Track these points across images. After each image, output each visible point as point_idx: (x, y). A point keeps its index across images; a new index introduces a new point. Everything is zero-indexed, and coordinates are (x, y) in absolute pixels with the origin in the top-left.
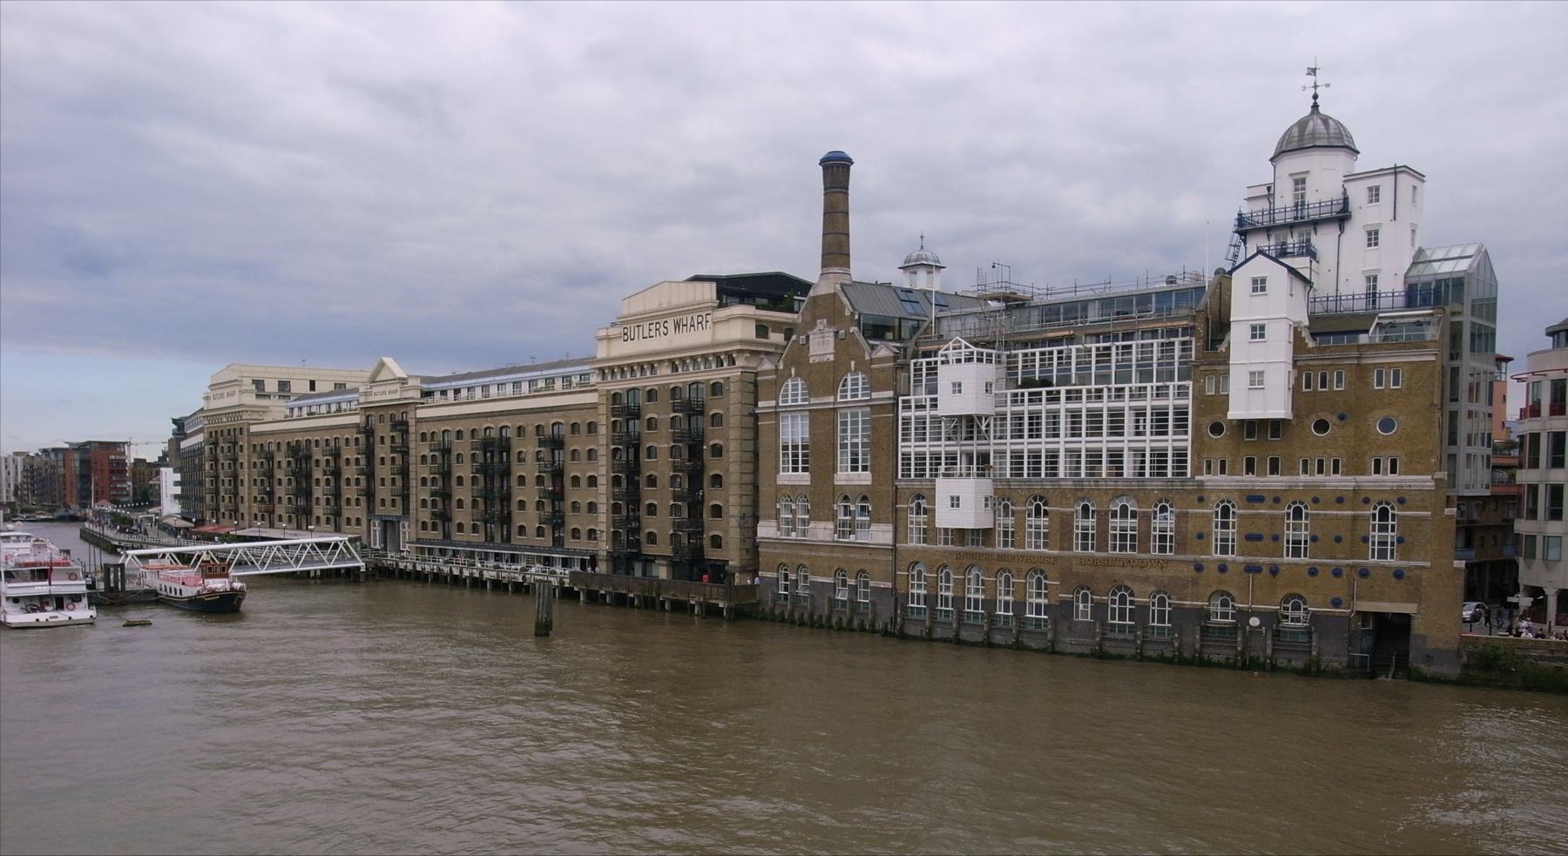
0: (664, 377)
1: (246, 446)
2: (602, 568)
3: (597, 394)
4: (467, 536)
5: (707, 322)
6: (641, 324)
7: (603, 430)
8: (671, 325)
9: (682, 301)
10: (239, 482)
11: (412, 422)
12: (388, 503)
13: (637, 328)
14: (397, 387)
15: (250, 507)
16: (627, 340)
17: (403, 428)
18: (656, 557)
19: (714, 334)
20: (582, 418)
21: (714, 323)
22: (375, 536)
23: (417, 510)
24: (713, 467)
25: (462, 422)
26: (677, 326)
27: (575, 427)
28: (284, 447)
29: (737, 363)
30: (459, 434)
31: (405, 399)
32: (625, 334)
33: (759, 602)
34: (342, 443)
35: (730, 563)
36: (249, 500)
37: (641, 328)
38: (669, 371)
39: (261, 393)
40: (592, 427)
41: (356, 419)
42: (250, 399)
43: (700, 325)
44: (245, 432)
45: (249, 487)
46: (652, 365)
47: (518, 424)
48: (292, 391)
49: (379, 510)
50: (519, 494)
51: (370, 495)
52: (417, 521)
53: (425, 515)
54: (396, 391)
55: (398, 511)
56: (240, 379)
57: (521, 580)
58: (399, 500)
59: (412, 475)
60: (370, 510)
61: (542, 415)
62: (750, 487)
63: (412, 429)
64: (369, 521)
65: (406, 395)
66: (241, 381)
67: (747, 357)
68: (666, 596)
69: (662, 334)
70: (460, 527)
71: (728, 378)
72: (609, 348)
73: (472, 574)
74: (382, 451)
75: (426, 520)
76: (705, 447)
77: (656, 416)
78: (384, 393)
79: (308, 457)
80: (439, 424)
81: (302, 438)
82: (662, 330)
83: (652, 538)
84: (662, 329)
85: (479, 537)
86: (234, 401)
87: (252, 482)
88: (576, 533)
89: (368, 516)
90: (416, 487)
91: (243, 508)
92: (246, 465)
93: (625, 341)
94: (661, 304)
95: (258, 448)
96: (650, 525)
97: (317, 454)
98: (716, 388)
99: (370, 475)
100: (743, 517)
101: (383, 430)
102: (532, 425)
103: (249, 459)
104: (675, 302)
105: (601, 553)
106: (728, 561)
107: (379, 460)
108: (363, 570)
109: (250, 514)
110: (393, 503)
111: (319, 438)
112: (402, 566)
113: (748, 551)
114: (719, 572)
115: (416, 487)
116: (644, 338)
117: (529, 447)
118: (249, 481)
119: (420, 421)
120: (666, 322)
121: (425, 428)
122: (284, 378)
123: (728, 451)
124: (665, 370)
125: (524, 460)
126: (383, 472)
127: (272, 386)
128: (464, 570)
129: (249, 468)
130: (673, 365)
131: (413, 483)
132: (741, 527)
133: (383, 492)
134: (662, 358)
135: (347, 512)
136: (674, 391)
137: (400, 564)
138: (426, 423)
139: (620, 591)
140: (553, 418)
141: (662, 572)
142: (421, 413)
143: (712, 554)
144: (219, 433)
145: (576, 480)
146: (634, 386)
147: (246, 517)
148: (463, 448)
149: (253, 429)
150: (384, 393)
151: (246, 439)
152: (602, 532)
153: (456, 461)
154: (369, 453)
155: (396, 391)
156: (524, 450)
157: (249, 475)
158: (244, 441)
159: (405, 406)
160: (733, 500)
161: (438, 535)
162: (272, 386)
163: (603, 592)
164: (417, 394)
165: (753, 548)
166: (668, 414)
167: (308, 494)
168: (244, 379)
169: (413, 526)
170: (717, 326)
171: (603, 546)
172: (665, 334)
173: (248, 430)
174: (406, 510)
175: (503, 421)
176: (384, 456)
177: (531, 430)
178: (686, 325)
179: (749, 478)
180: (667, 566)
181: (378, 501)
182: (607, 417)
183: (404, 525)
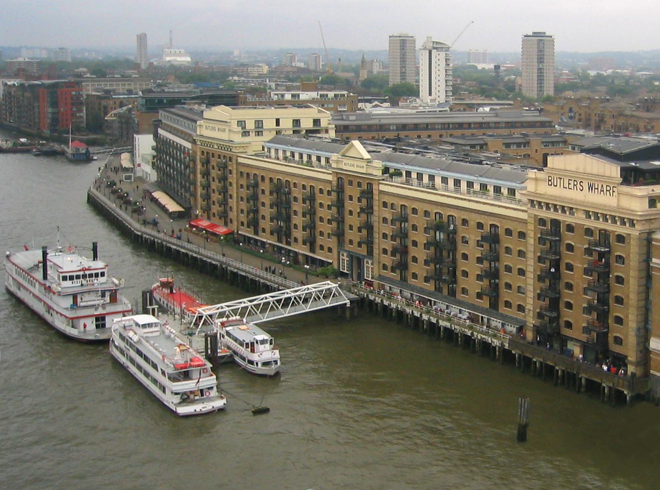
0: (578, 219)
1: (234, 171)
2: (530, 335)
3: (527, 214)
4: (419, 283)
5: (613, 192)
6: (563, 177)
7: (531, 241)
8: (585, 186)
9: (595, 172)
10: (229, 197)
11: (375, 192)
13: (559, 180)
15: (238, 216)
16: (551, 185)
17: (370, 196)
18: (572, 339)
19: (618, 201)
20: (516, 228)
21: (618, 194)
22: (343, 263)
23: (379, 254)
24: (617, 290)
25: (417, 203)
26: (591, 187)
27: (509, 232)
28: (267, 181)
29: (636, 227)
30: (415, 211)
31: (369, 174)
33: (648, 392)
34: (317, 191)
35: (629, 358)
36: (237, 211)
37: (562, 180)
39: (246, 133)
40: (522, 235)
41: (330, 178)
42: (238, 138)
43: (608, 192)
44: (234, 161)
45: (237, 202)
46: (571, 209)
47: (462, 217)
48: (264, 128)
49: (348, 247)
50: (462, 265)
51: (340, 235)
52: (379, 263)
53: (388, 260)
54: (363, 167)
55: (363, 251)
56: (229, 121)
57: (470, 335)
59: (376, 229)
61: (483, 216)
62: (644, 309)
63: (376, 197)
64: (339, 253)
65: (370, 171)
66: (230, 123)
67: (643, 224)
68: (582, 375)
69: (578, 189)
70: (415, 276)
71: (629, 234)
72: (536, 186)
73: (429, 319)
74: (353, 205)
75: (386, 263)
76: (611, 276)
77: (573, 244)
79: (289, 193)
81: (284, 179)
83: (569, 325)
85: (430, 286)
86: (224, 136)
87: (240, 199)
88: (508, 304)
89: (338, 249)
90: (379, 238)
91: (233, 215)
92: (235, 185)
93: (549, 185)
94: (577, 169)
95: (245, 175)
96: (567, 315)
97: (297, 193)
98: (621, 238)
99: (340, 220)
100: (639, 329)
101: (352, 191)
102: (474, 221)
103: (237, 182)
104: (588, 170)
105: (528, 324)
106: (627, 357)
107: (348, 212)
108: (348, 305)
109: (238, 221)
110: (360, 245)
111: (297, 182)
112: (372, 297)
113: (641, 352)
114: (620, 361)
115: (379, 238)
116: (564, 187)
117: (474, 236)
118: (237, 197)
119: (381, 192)
120: (582, 182)
121: (386, 199)
122: (259, 118)
123: (628, 282)
125: (467, 242)
126: (353, 220)
127: (250, 125)
128: (423, 315)
129: (237, 188)
130: (587, 213)
131: (376, 235)
132: (637, 336)
133: (353, 235)
134: (578, 208)
135: (320, 240)
136: (589, 232)
137: (370, 296)
138: (386, 196)
139: (549, 363)
140: (490, 220)
141: (577, 351)
142: (382, 188)
143: (614, 348)
144: (211, 155)
145: (508, 269)
147: (235, 223)
149: (240, 160)
150: (353, 165)
151: (235, 166)
152: (530, 310)
153: (411, 229)
154: (340, 204)
155: (363, 167)
156: (468, 237)
157: (237, 193)
158: (232, 166)
160: (631, 317)
161: (396, 276)
162: (250, 125)
163: (535, 360)
165: (645, 352)
166: (584, 244)
167: (288, 219)
168: (232, 121)
169: (376, 266)
170: (621, 196)
171: (531, 321)
172: (582, 190)
173: (237, 160)
174: (370, 253)
175: (450, 211)
177: (472, 224)
178: (595, 189)
179: (642, 303)
180: (580, 347)
181: (347, 241)
182: (535, 233)
183: (367, 262)
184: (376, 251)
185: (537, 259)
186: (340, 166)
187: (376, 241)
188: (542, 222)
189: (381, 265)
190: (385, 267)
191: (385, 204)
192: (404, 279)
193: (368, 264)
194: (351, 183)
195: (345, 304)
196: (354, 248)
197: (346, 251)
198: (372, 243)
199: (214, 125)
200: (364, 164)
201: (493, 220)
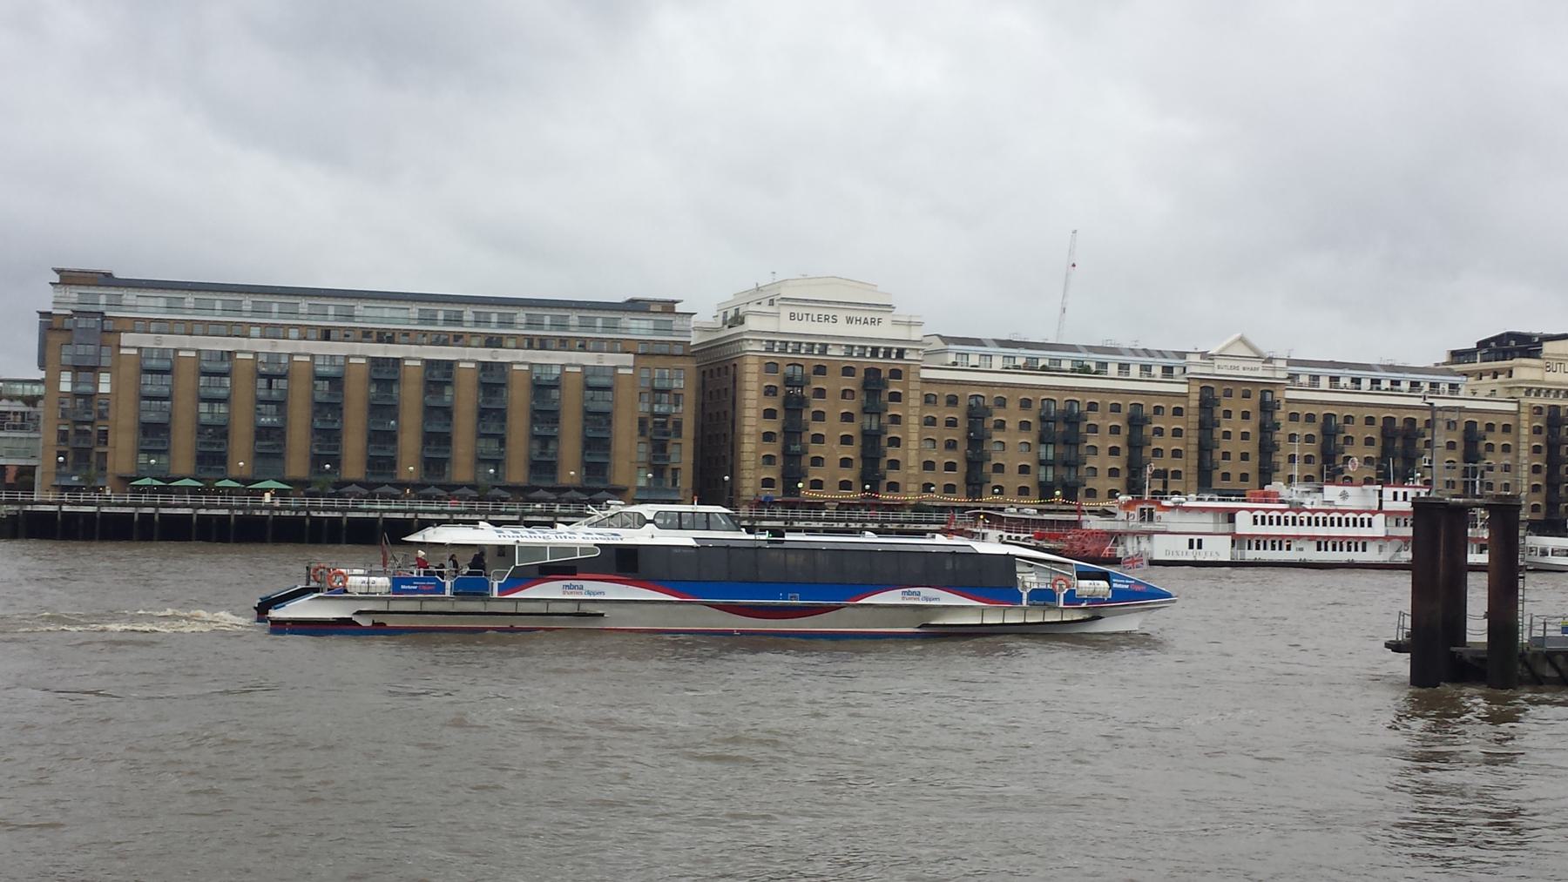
20: (1499, 421)
27: (1490, 427)
28: (1013, 405)
32: (1548, 367)
41: (1184, 389)
54: (1257, 369)
78: (1237, 368)
80: (1321, 407)
119: (1289, 401)
121: (1296, 409)
146: (1555, 404)
148: (1358, 431)
149: (925, 374)
150: (1237, 368)
159: (1267, 388)
175: (1406, 413)
176: (1248, 430)
185: (1531, 450)
188: (1539, 410)
191: (1294, 417)
194: (1228, 393)
199: (831, 313)
201: (1470, 417)
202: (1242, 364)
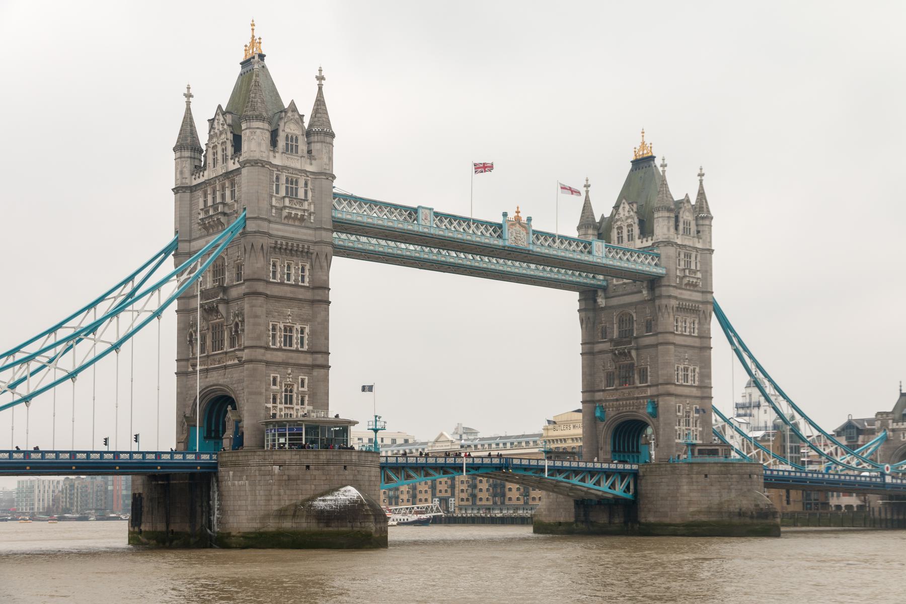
4: (484, 502)
8: (572, 426)
12: (443, 491)
14: (449, 444)
26: (574, 427)
38: (571, 442)
46: (565, 440)
49: (438, 494)
53: (464, 496)
55: (449, 494)
58: (449, 490)
60: (434, 495)
65: (453, 447)
82: (569, 428)
84: (569, 428)
110: (446, 491)
124: (570, 441)
130: (572, 439)
131: (457, 483)
135: (419, 496)
164: (459, 447)
174: (453, 495)
181: (438, 491)
183: (451, 501)
184: (456, 492)
186: (434, 448)
187: (457, 486)
189: (460, 500)
190: (462, 500)
192: (474, 504)
193: (452, 501)
195: (442, 515)
196: (444, 495)
197: (437, 497)
198: (454, 488)
200: (449, 444)
202: (444, 444)
